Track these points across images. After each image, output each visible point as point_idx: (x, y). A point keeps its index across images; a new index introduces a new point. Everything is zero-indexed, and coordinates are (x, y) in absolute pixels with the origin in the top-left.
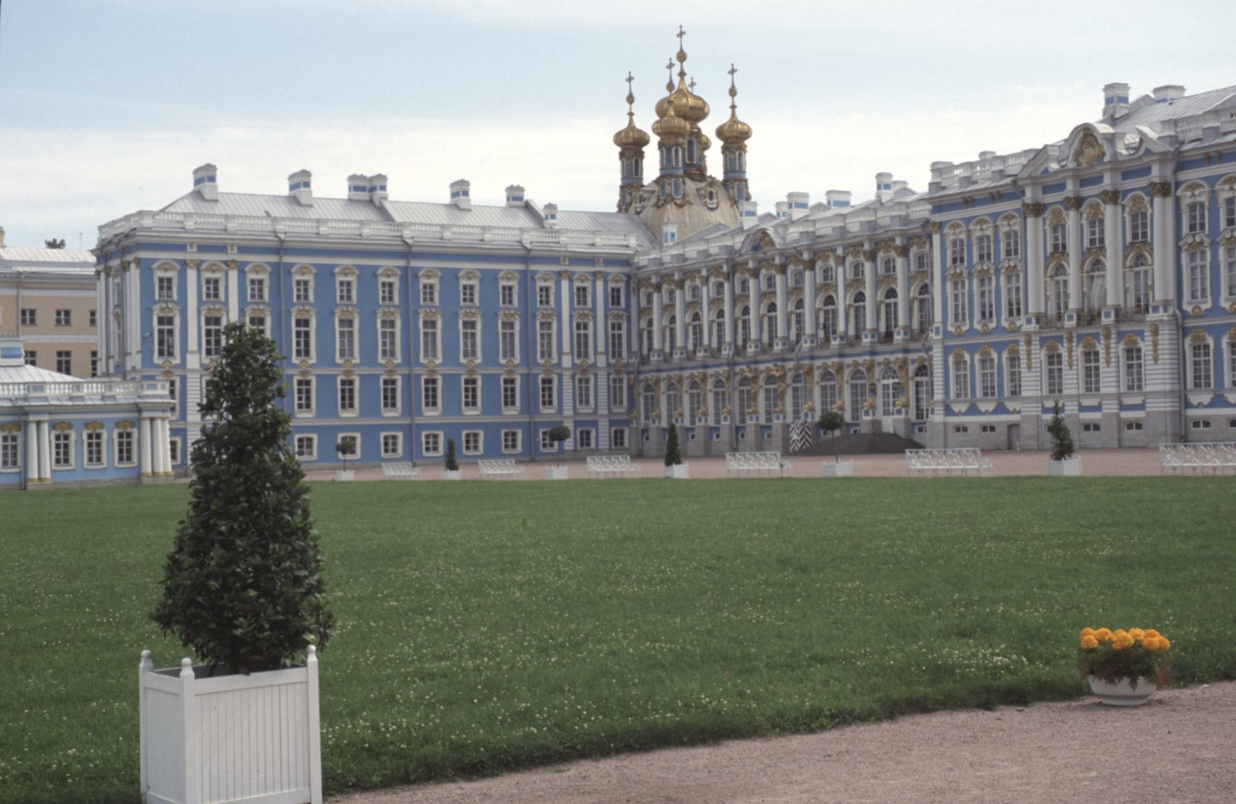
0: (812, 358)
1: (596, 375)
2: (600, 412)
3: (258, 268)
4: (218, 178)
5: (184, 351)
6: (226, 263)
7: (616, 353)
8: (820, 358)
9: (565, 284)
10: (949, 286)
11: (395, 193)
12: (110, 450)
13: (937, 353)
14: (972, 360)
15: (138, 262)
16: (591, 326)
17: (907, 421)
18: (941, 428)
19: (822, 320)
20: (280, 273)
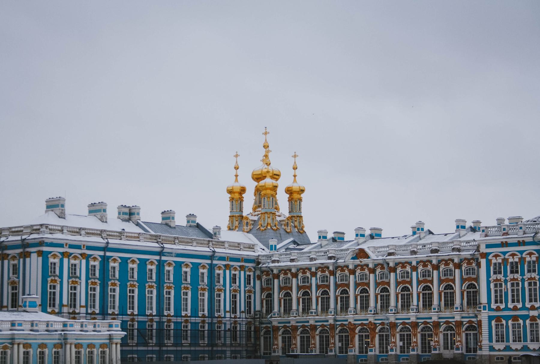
6: (81, 255)
9: (228, 272)
10: (492, 286)
11: (144, 216)
14: (507, 323)
15: (40, 253)
20: (105, 260)
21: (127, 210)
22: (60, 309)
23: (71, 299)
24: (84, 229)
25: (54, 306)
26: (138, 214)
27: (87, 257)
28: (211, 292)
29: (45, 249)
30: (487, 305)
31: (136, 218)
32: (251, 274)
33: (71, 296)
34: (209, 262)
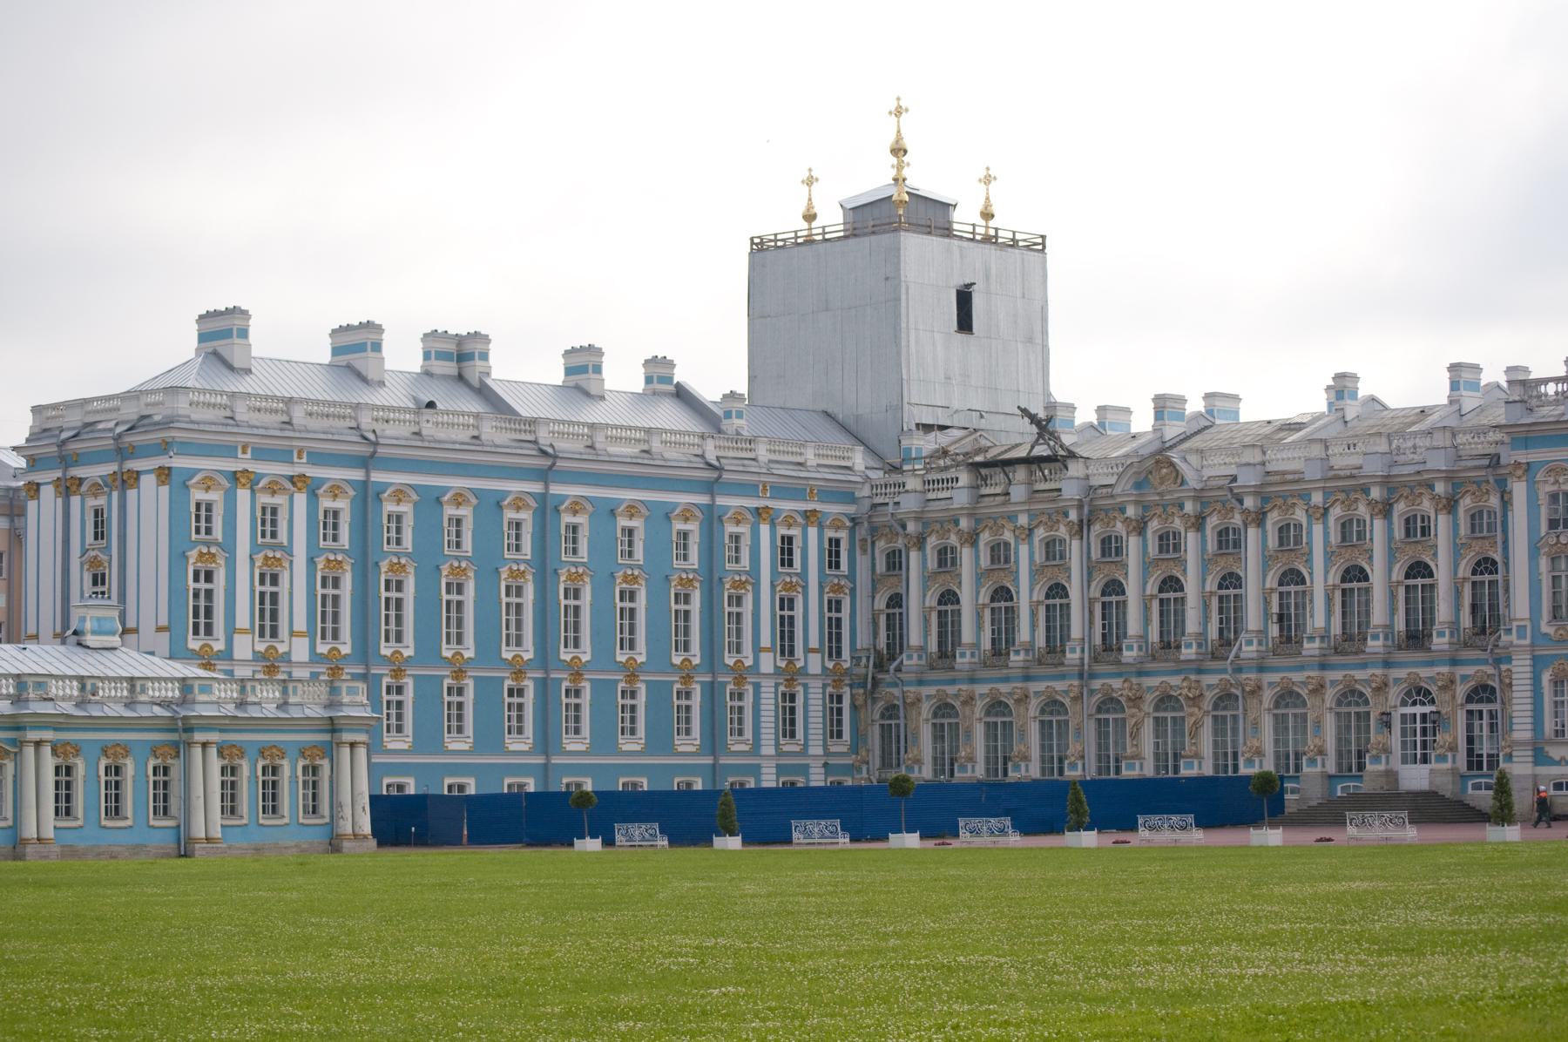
0: (1261, 669)
1: (805, 686)
2: (812, 751)
3: (336, 490)
4: (252, 331)
5: (231, 630)
6: (291, 479)
7: (787, 649)
8: (1401, 665)
9: (765, 529)
10: (1544, 564)
12: (293, 794)
13: (1521, 668)
15: (164, 474)
16: (799, 604)
17: (1454, 771)
18: (1530, 785)
19: (1275, 609)
21: (451, 347)
22: (229, 642)
23: (262, 611)
24: (302, 401)
25: (209, 630)
26: (484, 356)
27: (312, 489)
28: (711, 590)
29: (179, 462)
30: (1528, 623)
31: (478, 369)
32: (843, 535)
33: (262, 602)
34: (703, 499)
